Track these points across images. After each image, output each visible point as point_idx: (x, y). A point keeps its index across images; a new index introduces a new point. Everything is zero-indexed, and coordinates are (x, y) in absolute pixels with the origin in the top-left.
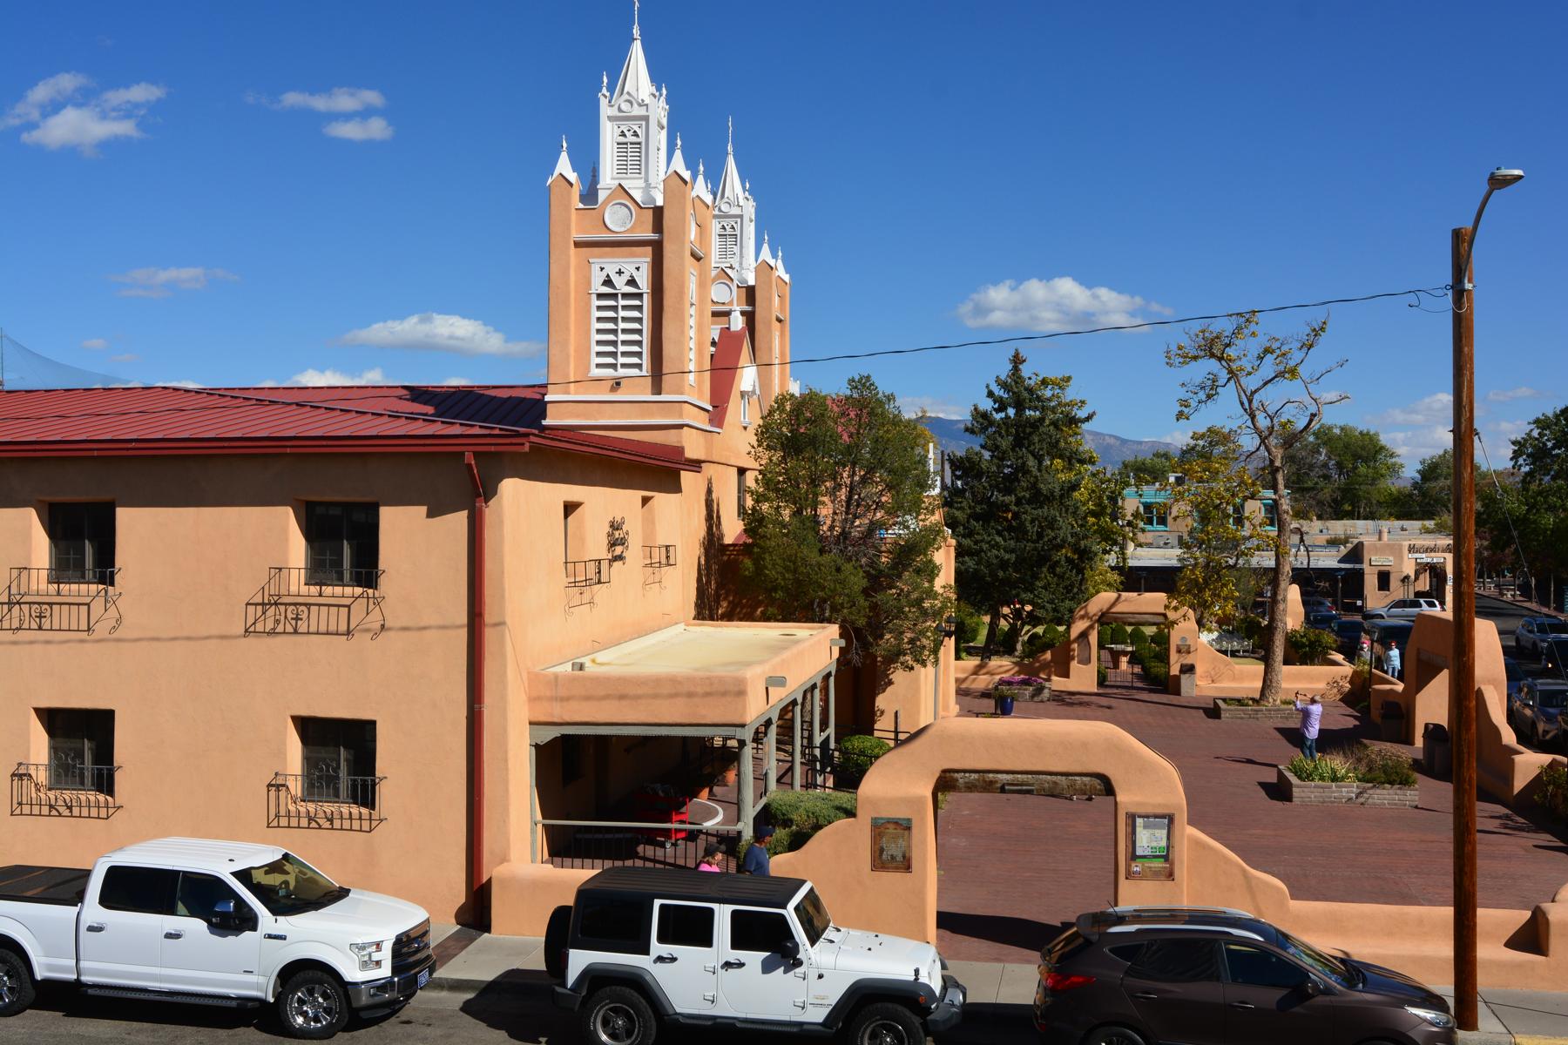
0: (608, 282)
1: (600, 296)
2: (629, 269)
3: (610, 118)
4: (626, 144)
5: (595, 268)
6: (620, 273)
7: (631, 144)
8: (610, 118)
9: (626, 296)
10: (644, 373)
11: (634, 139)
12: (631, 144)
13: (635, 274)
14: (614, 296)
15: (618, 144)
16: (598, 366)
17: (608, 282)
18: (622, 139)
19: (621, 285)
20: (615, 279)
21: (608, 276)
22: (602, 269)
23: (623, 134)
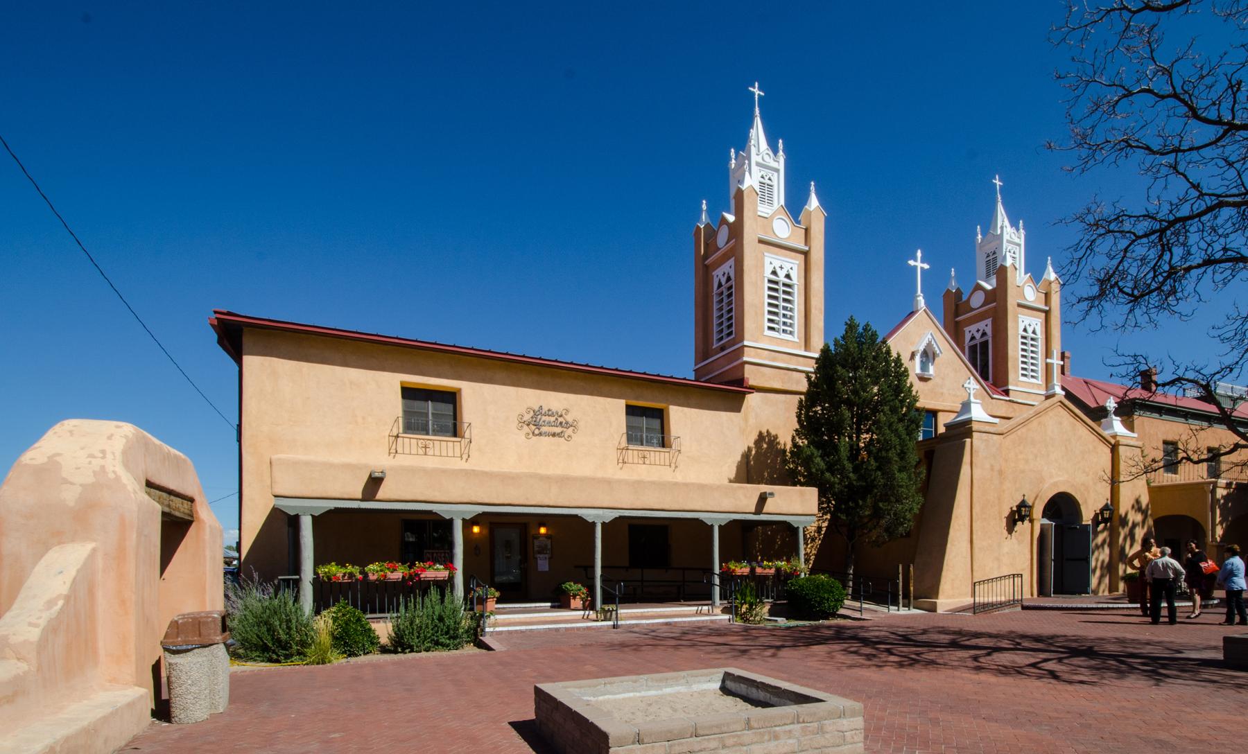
0: (774, 273)
1: (770, 281)
2: (787, 266)
3: (758, 164)
4: (764, 184)
5: (767, 260)
6: (781, 268)
7: (768, 185)
8: (758, 164)
9: (785, 285)
10: (796, 340)
11: (769, 182)
12: (768, 185)
13: (790, 270)
14: (776, 283)
15: (760, 183)
16: (770, 328)
17: (774, 273)
18: (762, 180)
19: (782, 274)
20: (778, 270)
21: (774, 268)
22: (771, 263)
23: (762, 177)
